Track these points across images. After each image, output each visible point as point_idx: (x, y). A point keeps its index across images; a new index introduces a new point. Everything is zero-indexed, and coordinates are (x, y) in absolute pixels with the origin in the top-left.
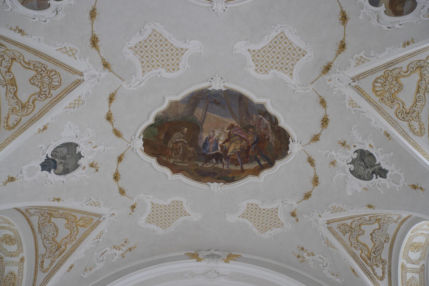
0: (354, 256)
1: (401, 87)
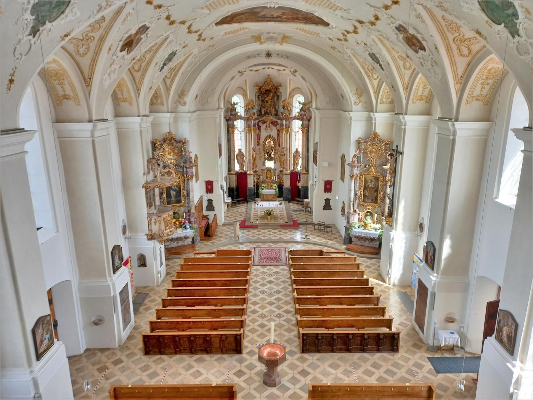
0: (363, 67)
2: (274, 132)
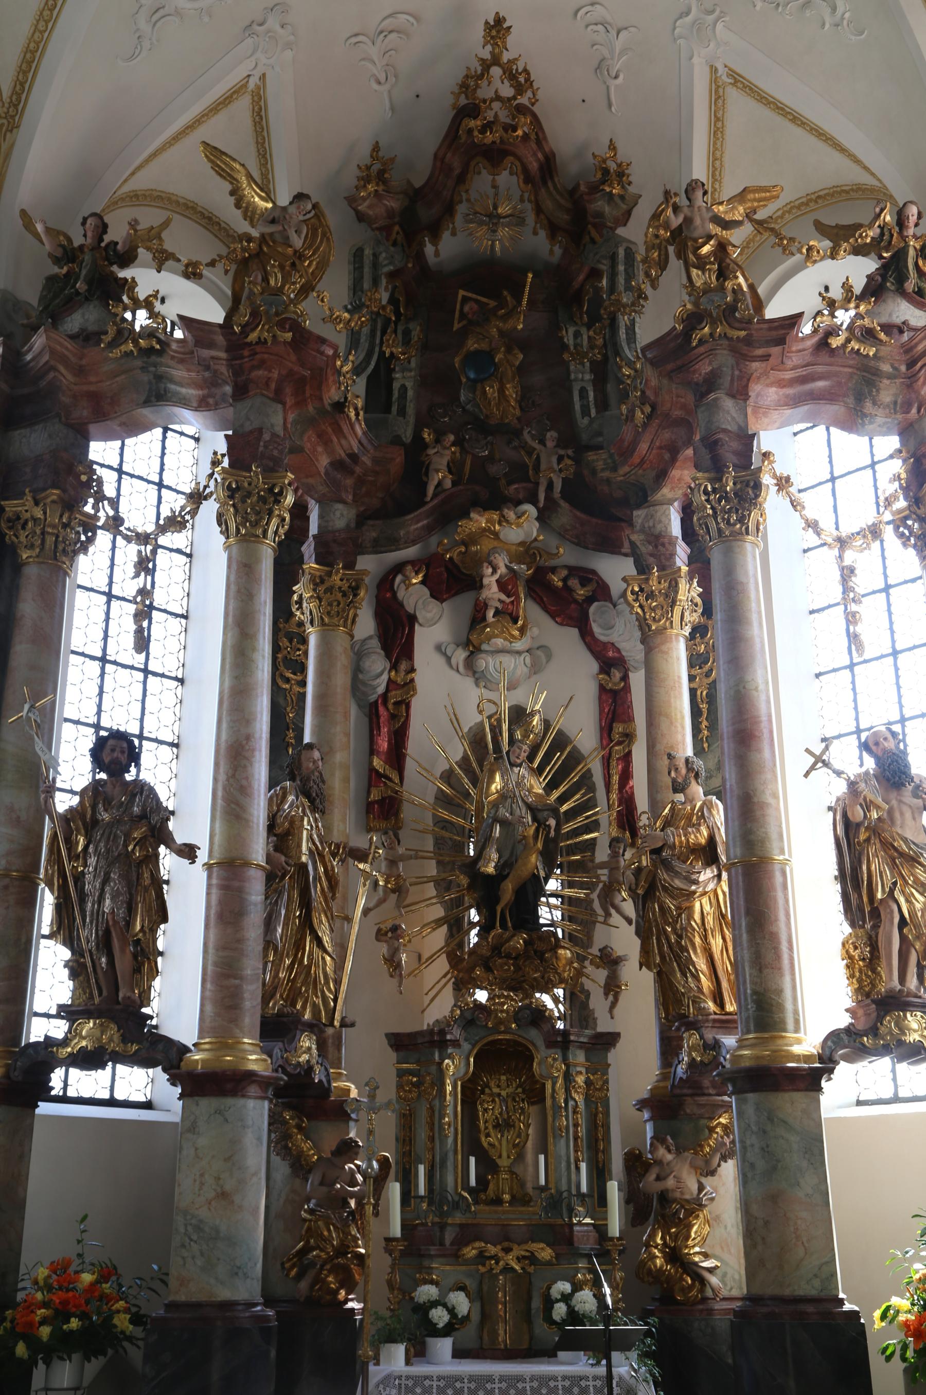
2: (555, 688)
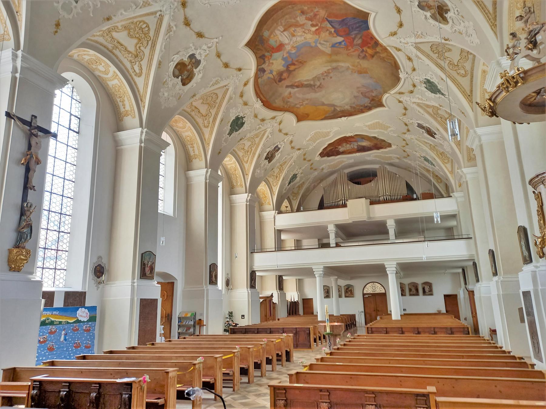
1: (131, 37)
